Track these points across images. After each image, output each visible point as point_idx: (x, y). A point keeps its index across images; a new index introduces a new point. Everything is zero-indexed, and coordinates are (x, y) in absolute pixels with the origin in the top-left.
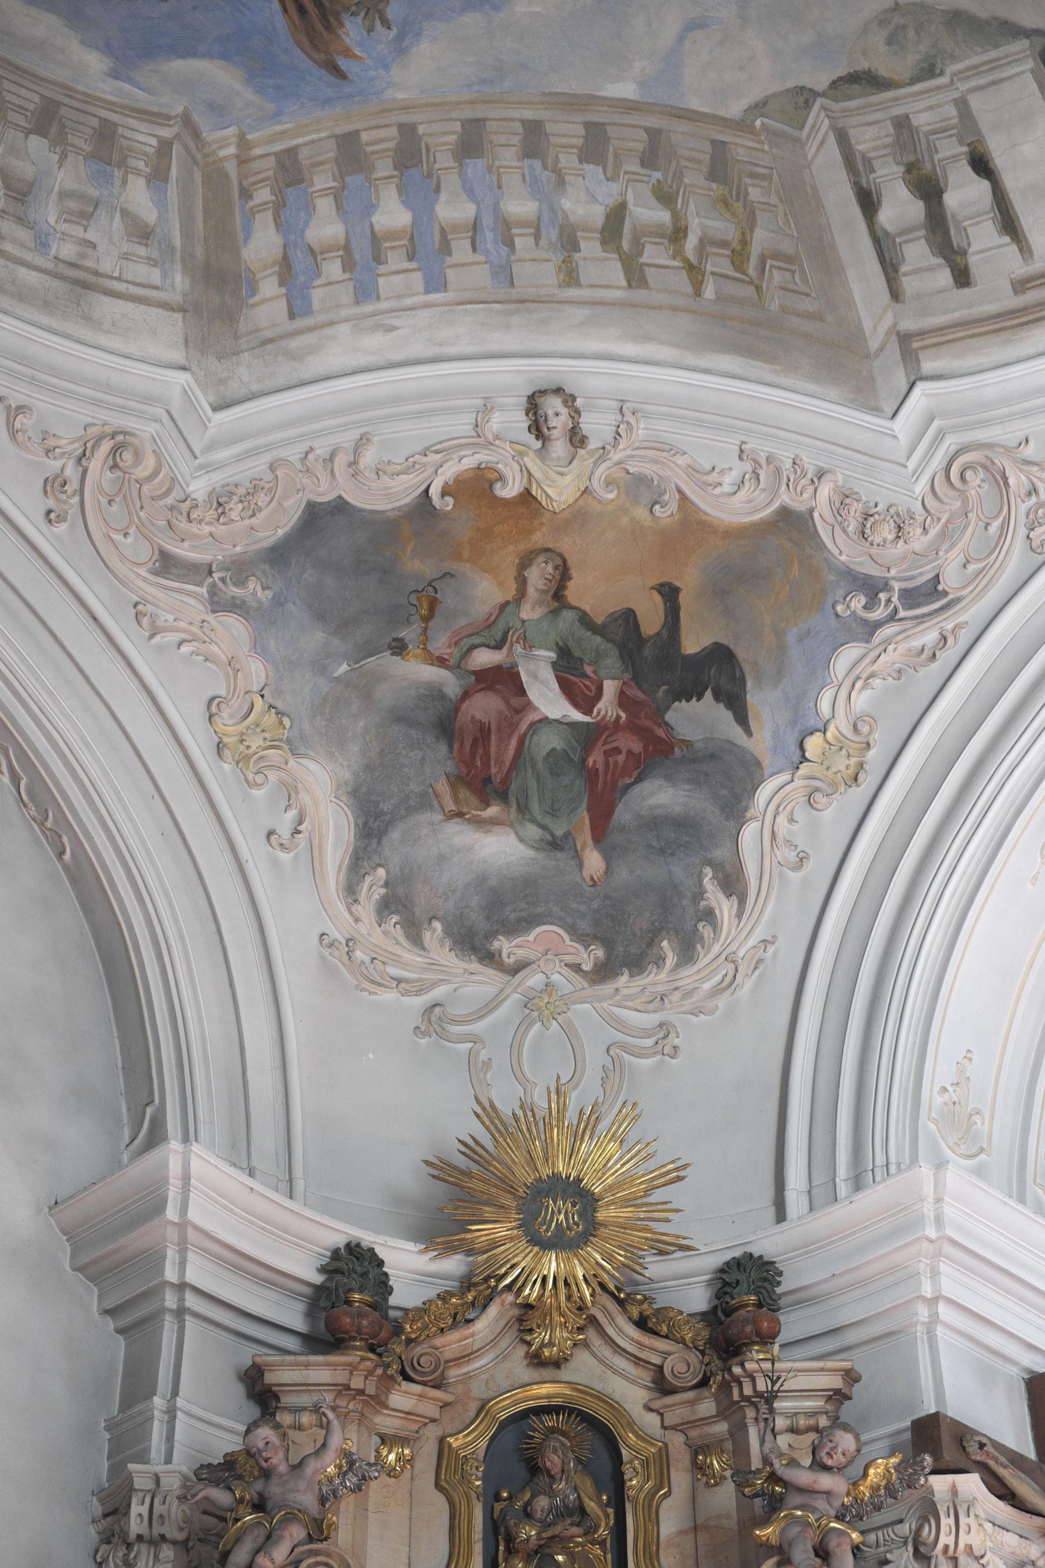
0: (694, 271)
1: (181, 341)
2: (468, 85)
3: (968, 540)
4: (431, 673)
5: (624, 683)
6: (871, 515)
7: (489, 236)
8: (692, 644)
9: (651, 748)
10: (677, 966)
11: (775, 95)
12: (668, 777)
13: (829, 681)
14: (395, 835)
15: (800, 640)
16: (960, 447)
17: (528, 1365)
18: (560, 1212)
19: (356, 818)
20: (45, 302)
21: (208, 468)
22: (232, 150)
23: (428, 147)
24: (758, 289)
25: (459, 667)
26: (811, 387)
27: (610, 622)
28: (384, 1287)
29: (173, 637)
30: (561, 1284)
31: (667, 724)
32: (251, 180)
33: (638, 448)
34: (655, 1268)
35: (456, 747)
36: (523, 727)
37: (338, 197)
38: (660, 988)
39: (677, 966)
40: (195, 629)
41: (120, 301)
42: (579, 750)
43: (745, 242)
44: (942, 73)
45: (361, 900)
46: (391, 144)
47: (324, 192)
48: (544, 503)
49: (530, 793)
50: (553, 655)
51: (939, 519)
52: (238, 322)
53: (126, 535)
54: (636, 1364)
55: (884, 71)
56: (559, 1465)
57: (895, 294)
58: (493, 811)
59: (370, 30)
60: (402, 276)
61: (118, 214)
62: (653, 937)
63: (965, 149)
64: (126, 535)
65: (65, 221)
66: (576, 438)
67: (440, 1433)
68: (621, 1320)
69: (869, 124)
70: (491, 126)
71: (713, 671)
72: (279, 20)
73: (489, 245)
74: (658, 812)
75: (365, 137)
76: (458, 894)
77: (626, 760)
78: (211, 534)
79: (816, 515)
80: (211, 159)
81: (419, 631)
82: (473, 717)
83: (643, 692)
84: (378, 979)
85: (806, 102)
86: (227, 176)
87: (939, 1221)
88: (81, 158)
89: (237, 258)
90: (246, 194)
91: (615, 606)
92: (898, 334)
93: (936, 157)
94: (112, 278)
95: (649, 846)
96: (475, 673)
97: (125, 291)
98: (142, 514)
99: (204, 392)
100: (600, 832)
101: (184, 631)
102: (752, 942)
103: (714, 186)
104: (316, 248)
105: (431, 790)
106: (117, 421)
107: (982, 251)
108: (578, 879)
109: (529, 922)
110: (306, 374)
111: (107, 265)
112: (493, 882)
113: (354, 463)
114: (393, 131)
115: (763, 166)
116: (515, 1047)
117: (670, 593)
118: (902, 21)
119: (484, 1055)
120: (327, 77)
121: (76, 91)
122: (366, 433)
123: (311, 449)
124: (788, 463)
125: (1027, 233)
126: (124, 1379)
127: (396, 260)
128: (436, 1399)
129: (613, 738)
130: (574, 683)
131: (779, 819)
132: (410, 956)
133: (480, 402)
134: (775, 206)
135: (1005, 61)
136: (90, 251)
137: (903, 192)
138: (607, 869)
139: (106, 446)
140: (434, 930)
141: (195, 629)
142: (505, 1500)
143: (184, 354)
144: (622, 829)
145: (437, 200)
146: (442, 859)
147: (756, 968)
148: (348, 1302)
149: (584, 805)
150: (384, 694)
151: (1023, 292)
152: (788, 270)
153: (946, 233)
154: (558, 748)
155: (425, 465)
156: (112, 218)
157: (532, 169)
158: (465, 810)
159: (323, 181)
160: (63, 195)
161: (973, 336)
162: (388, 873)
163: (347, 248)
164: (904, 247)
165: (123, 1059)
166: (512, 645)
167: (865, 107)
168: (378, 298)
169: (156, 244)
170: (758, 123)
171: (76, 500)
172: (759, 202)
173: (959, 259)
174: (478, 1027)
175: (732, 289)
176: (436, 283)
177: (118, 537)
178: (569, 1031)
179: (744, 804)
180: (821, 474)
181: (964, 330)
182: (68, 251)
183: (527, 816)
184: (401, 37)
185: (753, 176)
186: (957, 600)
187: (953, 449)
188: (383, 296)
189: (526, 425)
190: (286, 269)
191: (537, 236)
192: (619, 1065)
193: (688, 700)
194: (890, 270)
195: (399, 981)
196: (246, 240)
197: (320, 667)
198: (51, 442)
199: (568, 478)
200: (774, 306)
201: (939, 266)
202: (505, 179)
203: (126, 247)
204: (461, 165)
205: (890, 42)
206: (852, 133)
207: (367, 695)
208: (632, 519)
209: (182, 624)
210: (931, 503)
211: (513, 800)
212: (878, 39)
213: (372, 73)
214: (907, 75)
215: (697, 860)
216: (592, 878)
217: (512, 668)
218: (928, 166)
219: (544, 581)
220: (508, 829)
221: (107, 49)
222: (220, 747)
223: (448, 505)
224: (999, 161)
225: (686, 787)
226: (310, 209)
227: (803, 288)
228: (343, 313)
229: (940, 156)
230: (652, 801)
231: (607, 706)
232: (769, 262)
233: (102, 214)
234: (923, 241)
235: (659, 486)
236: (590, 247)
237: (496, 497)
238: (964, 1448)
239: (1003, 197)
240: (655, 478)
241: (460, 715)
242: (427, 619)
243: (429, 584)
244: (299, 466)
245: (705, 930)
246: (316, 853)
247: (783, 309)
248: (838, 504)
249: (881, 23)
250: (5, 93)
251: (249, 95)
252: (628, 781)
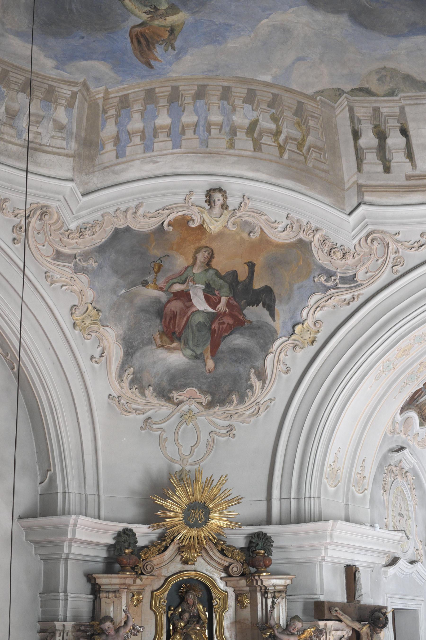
0: (281, 148)
1: (72, 168)
2: (203, 72)
3: (370, 265)
4: (156, 293)
5: (229, 298)
6: (334, 248)
7: (201, 128)
8: (257, 285)
9: (236, 323)
10: (237, 404)
11: (327, 89)
12: (241, 334)
13: (307, 305)
14: (138, 354)
15: (299, 288)
16: (373, 230)
17: (181, 563)
18: (197, 514)
19: (124, 349)
20: (18, 157)
21: (78, 218)
22: (102, 95)
23: (182, 95)
24: (306, 158)
25: (167, 291)
26: (319, 197)
27: (227, 275)
29: (59, 284)
30: (196, 540)
31: (244, 314)
32: (108, 106)
33: (247, 211)
35: (163, 320)
36: (189, 313)
37: (142, 113)
38: (231, 412)
39: (237, 404)
40: (68, 281)
41: (49, 155)
42: (209, 322)
43: (303, 140)
44: (397, 95)
45: (124, 380)
46: (168, 93)
47: (137, 111)
48: (208, 230)
49: (189, 338)
50: (204, 287)
51: (359, 254)
52: (95, 160)
53: (44, 246)
55: (374, 88)
57: (359, 169)
58: (175, 344)
59: (166, 50)
60: (164, 143)
61: (52, 121)
62: (230, 393)
63: (399, 125)
64: (44, 246)
66: (224, 206)
68: (215, 551)
69: (363, 107)
70: (209, 88)
71: (263, 296)
72: (129, 45)
73: (201, 132)
74: (236, 346)
75: (157, 90)
76: (159, 376)
77: (226, 327)
78: (76, 243)
79: (312, 244)
80: (92, 99)
81: (154, 277)
82: (171, 310)
83: (236, 302)
84: (128, 409)
85: (340, 94)
86: (98, 105)
87: (331, 536)
88: (39, 100)
89: (98, 134)
90: (105, 112)
91: (229, 269)
92: (358, 184)
93: (387, 125)
94: (46, 146)
95: (231, 359)
96: (173, 293)
97: (51, 150)
98: (50, 237)
100: (213, 353)
101: (64, 281)
102: (266, 399)
103: (296, 118)
104: (131, 132)
105: (152, 337)
106: (43, 202)
107: (397, 162)
108: (204, 370)
109: (184, 386)
110: (120, 179)
111: (45, 141)
112: (173, 371)
113: (135, 213)
114: (169, 89)
115: (317, 114)
116: (176, 433)
117: (251, 266)
118: (385, 74)
119: (165, 435)
120: (145, 67)
121: (40, 75)
122: (142, 202)
123: (119, 209)
124: (305, 223)
125: (416, 160)
127: (162, 137)
129: (222, 318)
130: (210, 297)
131: (281, 355)
132: (141, 400)
133: (187, 190)
134: (318, 129)
135: (423, 97)
136: (39, 136)
137: (371, 134)
138: (215, 367)
139: (39, 212)
140: (150, 390)
141: (68, 281)
143: (72, 174)
144: (222, 352)
145: (182, 115)
146: (154, 363)
147: (266, 409)
148: (125, 553)
149: (209, 343)
150: (138, 301)
151: (410, 180)
152: (319, 153)
153: (385, 153)
154: (202, 321)
155: (163, 214)
156: (49, 122)
157: (223, 104)
158: (164, 344)
159: (137, 107)
161: (386, 191)
163: (143, 132)
164: (367, 154)
165: (37, 449)
166: (188, 282)
167: (363, 101)
168: (153, 151)
169: (66, 132)
170: (318, 98)
172: (312, 127)
173: (387, 163)
175: (295, 156)
176: (177, 145)
177: (40, 247)
178: (196, 426)
179: (269, 346)
180: (317, 230)
181: (384, 189)
183: (187, 347)
184: (178, 54)
185: (312, 117)
186: (361, 285)
187: (370, 230)
188: (155, 150)
189: (205, 200)
190: (117, 140)
191: (221, 130)
192: (213, 440)
193: (253, 306)
194: (359, 161)
195: (136, 410)
196: (102, 129)
197: (114, 291)
198: (17, 212)
199: (219, 223)
200: (311, 165)
201: (379, 164)
202: (211, 107)
203: (53, 134)
204: (195, 102)
205: (378, 80)
206: (355, 109)
207: (131, 301)
208: (241, 237)
209: (63, 279)
210: (358, 248)
211: (183, 341)
212: (374, 78)
213: (165, 66)
214: (382, 93)
215: (249, 366)
216: (209, 370)
217: (187, 291)
218: (383, 127)
219: (204, 258)
220: (179, 351)
221: (56, 58)
222: (75, 325)
223: (170, 230)
224: (412, 132)
225: (248, 338)
226: (130, 117)
227: (323, 160)
228: (138, 156)
229: (388, 125)
230: (234, 342)
231: (222, 307)
232: (312, 149)
233: (45, 121)
234: (375, 154)
235: (253, 225)
236: (241, 135)
237: (189, 226)
238: (331, 612)
239: (410, 145)
240: (252, 223)
241: (166, 309)
242: (157, 273)
243: (159, 259)
244: (113, 214)
245: (249, 393)
246: (108, 364)
247: (314, 166)
248: (322, 242)
249: (377, 72)
250: (10, 77)
251: (112, 74)
252: (226, 334)
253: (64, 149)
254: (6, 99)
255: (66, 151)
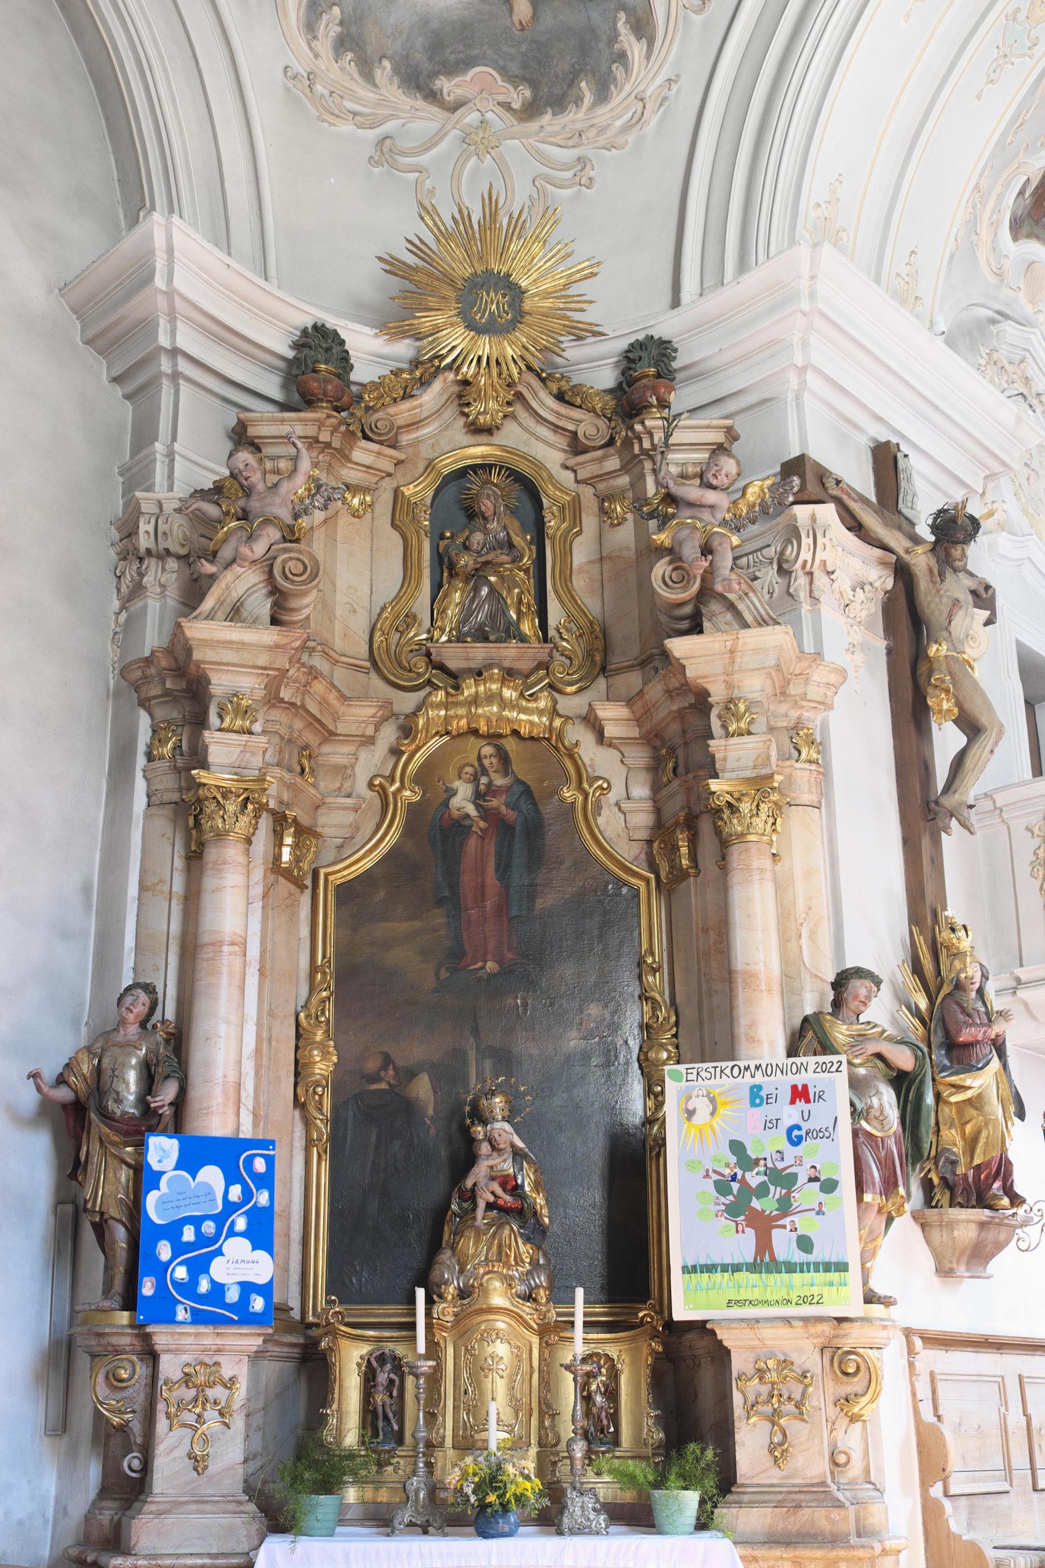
10: (594, 105)
17: (466, 433)
18: (492, 302)
28: (344, 361)
30: (493, 364)
34: (573, 352)
38: (579, 126)
39: (594, 105)
45: (320, 36)
54: (555, 431)
56: (492, 509)
62: (572, 79)
67: (395, 485)
68: (543, 394)
76: (404, 36)
84: (336, 111)
87: (812, 296)
102: (658, 81)
108: (508, 23)
112: (435, 24)
119: (428, 184)
126: (132, 436)
128: (391, 457)
132: (364, 91)
138: (534, 14)
140: (384, 69)
142: (448, 538)
147: (661, 105)
148: (315, 371)
162: (342, 13)
165: (118, 172)
174: (424, 159)
192: (542, 193)
195: (355, 114)
215: (613, 6)
216: (521, 23)
238: (823, 485)
245: (618, 71)
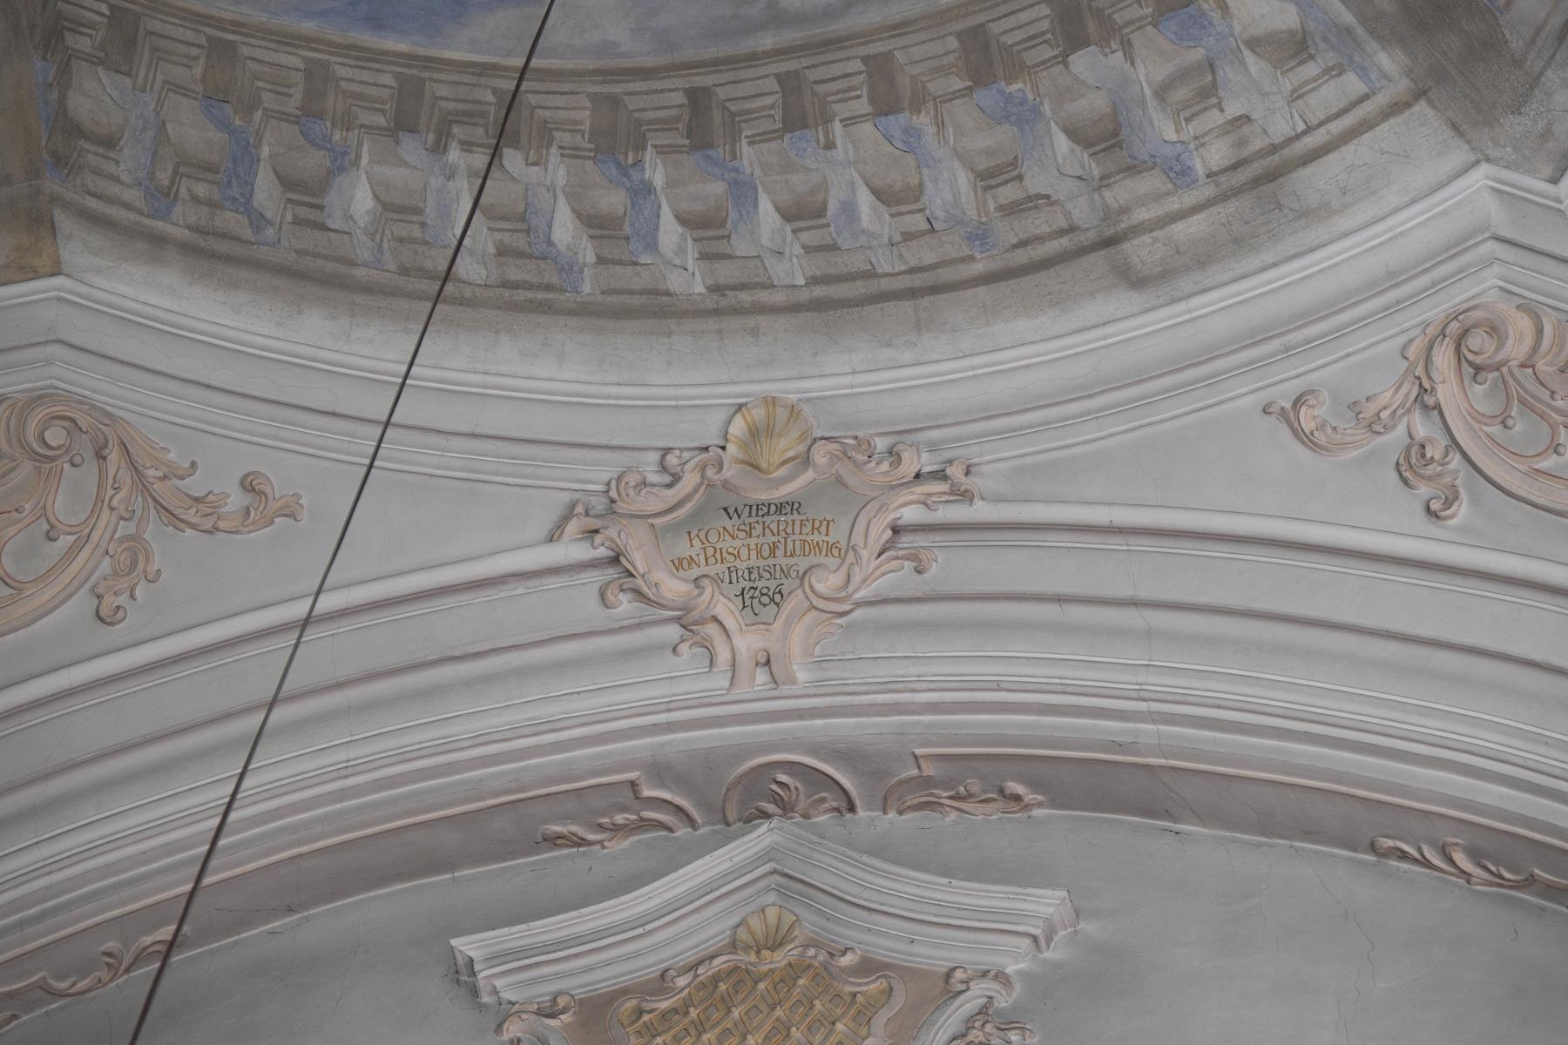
41: (1330, 157)
52: (1506, 42)
61: (1246, 53)
65: (1187, 120)
88: (1150, 28)
94: (1298, 136)
97: (1327, 138)
98: (1560, 403)
99: (1532, 172)
106: (1435, 310)
111: (1280, 127)
136: (1246, 129)
139: (1443, 357)
143: (1466, 147)
156: (1243, 63)
160: (1161, 92)
169: (1322, 45)
171: (1456, 461)
182: (1218, 154)
198: (1369, 411)
233: (1227, 71)
250: (1003, 39)
253: (1365, 98)
254: (1047, 108)
255: (1381, 100)
